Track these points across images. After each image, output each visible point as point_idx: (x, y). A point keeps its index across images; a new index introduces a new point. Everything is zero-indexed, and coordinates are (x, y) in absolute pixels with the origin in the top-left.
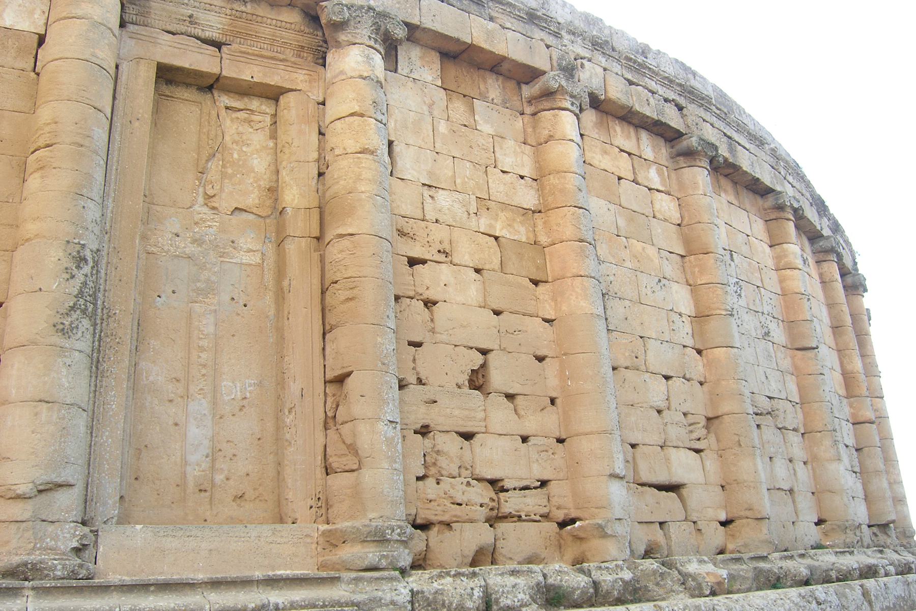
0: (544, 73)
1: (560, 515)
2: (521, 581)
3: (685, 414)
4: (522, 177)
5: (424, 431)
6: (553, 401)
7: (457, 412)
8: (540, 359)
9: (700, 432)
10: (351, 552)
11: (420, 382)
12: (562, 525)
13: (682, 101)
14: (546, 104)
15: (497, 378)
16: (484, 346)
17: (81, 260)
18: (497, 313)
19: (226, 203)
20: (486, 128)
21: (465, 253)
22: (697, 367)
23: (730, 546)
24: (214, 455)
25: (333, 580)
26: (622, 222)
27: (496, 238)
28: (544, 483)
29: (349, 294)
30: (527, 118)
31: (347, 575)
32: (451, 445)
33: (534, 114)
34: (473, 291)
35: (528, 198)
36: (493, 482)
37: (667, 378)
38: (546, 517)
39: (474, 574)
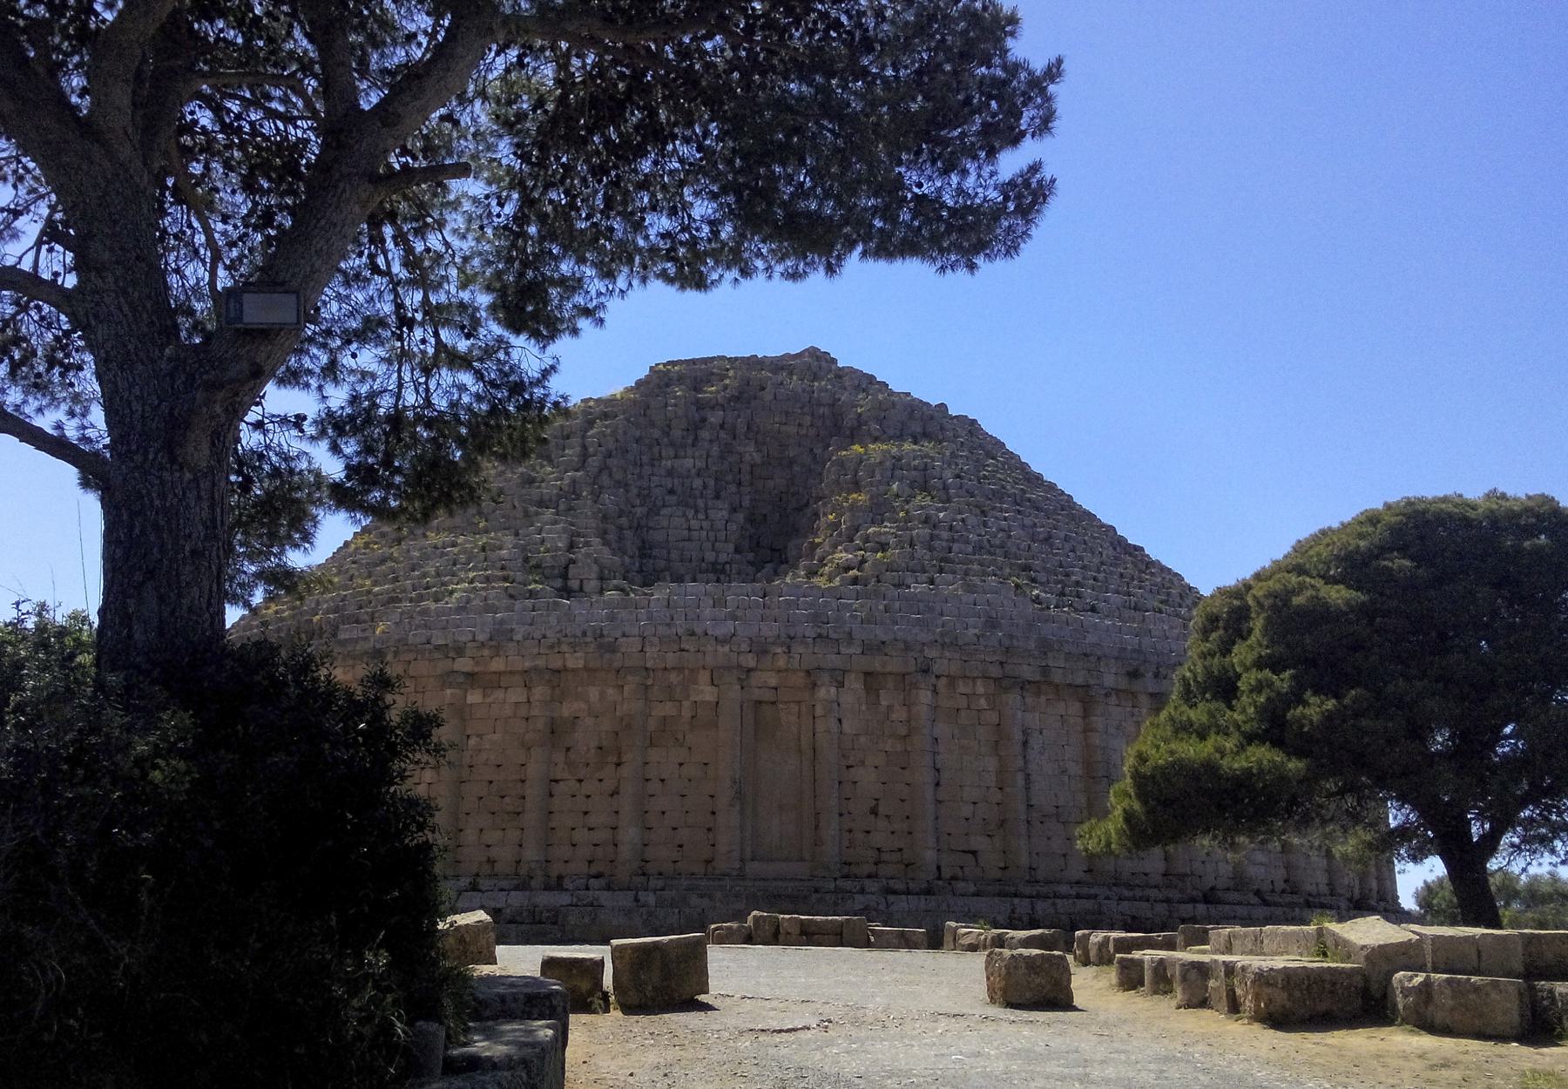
1: (906, 862)
2: (876, 884)
5: (850, 831)
8: (902, 801)
11: (849, 813)
12: (907, 866)
15: (881, 810)
16: (877, 797)
17: (735, 782)
20: (884, 703)
22: (998, 796)
28: (900, 850)
32: (860, 836)
35: (904, 732)
36: (878, 849)
37: (975, 803)
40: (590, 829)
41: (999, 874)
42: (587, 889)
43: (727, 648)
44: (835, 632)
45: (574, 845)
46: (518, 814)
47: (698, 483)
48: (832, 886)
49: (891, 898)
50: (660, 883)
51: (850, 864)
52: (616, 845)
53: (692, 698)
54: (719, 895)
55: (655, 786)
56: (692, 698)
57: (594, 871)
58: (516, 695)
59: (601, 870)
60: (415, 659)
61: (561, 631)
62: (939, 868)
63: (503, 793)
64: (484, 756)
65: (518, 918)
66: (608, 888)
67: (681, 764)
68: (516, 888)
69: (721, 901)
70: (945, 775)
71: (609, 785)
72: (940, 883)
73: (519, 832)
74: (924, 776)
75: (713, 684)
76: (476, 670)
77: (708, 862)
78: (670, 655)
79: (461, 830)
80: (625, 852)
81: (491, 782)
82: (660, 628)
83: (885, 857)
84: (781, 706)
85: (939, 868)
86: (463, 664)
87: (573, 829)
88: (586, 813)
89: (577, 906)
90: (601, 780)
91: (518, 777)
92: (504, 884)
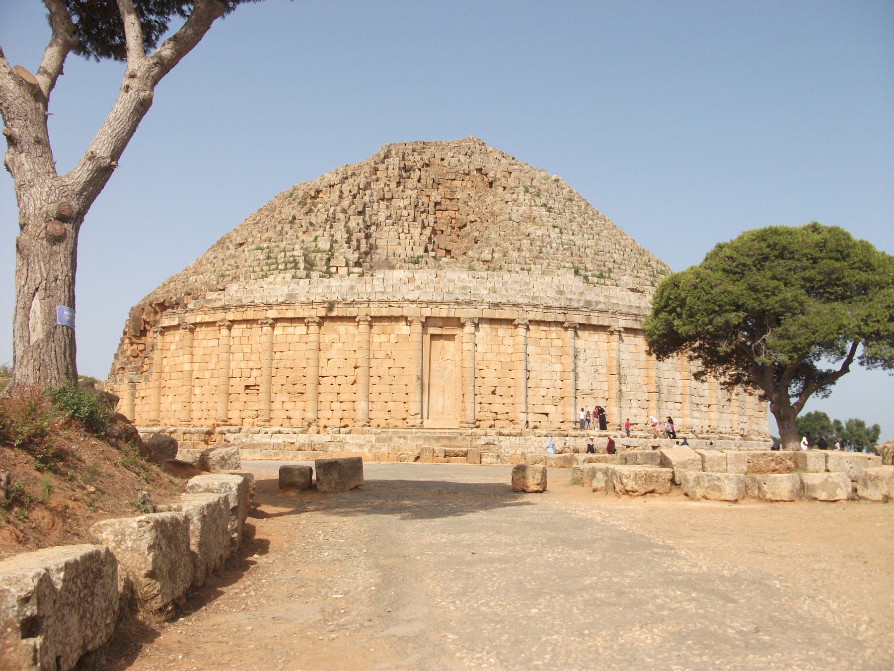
0: (515, 320)
5: (481, 403)
9: (557, 401)
10: (464, 425)
13: (566, 312)
15: (497, 392)
21: (492, 366)
22: (559, 384)
24: (443, 407)
26: (539, 351)
32: (486, 406)
34: (494, 374)
36: (496, 413)
41: (560, 425)
42: (339, 433)
43: (415, 305)
46: (303, 394)
47: (405, 213)
48: (471, 431)
49: (501, 438)
50: (379, 430)
51: (480, 421)
53: (396, 332)
54: (409, 436)
55: (375, 380)
56: (396, 332)
57: (343, 424)
58: (301, 329)
61: (324, 296)
62: (527, 422)
64: (284, 362)
65: (303, 448)
66: (350, 432)
68: (302, 432)
70: (532, 375)
71: (352, 379)
72: (527, 430)
74: (521, 375)
77: (404, 419)
78: (384, 309)
80: (360, 415)
82: (378, 295)
83: (499, 417)
85: (527, 422)
86: (272, 314)
88: (338, 394)
92: (296, 430)
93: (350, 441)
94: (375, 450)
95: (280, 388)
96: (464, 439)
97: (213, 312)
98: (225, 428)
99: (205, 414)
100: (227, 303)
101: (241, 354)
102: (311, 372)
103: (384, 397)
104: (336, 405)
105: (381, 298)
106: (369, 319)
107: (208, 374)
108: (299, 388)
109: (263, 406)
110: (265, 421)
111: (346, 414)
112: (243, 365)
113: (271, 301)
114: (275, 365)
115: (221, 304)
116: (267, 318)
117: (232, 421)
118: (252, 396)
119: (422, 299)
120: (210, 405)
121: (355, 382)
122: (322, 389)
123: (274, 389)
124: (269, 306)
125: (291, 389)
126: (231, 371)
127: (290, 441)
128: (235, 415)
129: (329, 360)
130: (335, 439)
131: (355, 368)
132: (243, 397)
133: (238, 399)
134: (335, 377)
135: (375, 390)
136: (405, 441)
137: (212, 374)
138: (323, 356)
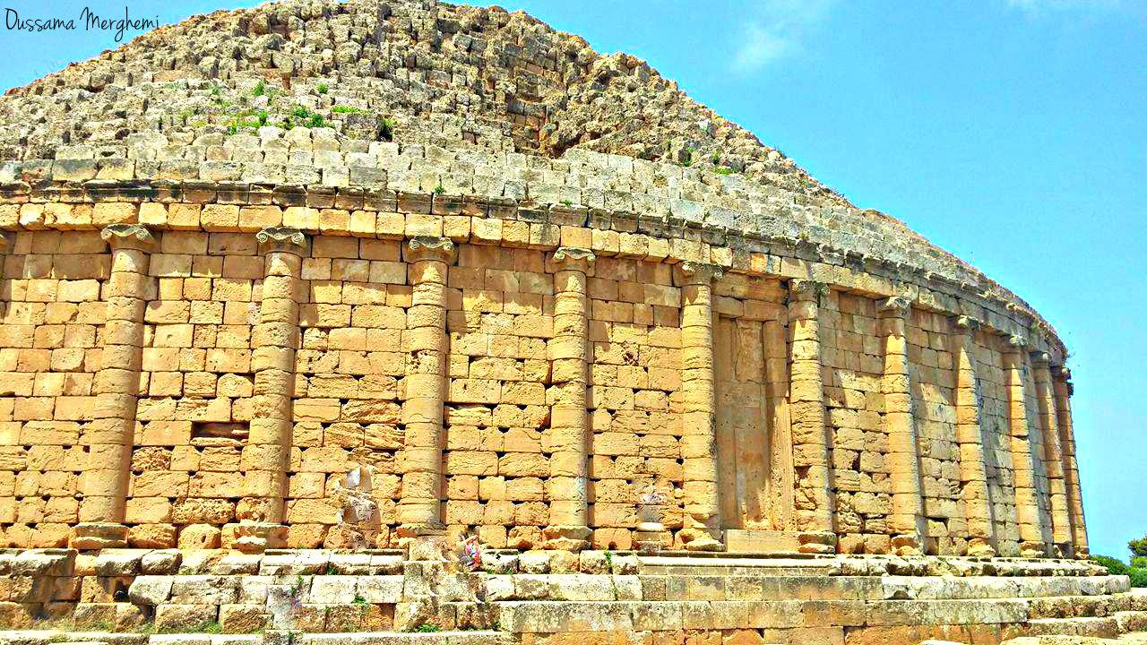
3: (950, 480)
4: (875, 356)
6: (888, 475)
7: (848, 482)
13: (959, 295)
14: (888, 315)
15: (863, 465)
16: (858, 449)
18: (864, 431)
19: (743, 379)
20: (859, 331)
23: (970, 551)
25: (813, 557)
27: (863, 392)
28: (884, 516)
29: (810, 430)
30: (878, 321)
31: (817, 555)
32: (845, 496)
33: (881, 319)
36: (864, 517)
38: (885, 532)
39: (863, 558)
40: (508, 478)
44: (815, 235)
45: (485, 502)
46: (392, 451)
52: (548, 503)
53: (647, 301)
54: (727, 578)
57: (513, 542)
59: (528, 539)
60: (214, 202)
63: (367, 418)
64: (329, 360)
67: (635, 391)
69: (732, 589)
71: (537, 414)
73: (394, 479)
75: (673, 285)
76: (324, 228)
77: (674, 529)
79: (294, 474)
80: (567, 516)
81: (344, 401)
84: (741, 325)
86: (302, 218)
87: (481, 477)
88: (500, 454)
89: (525, 599)
90: (522, 407)
91: (391, 396)
93: (572, 596)
94: (650, 624)
95: (317, 434)
96: (849, 586)
97: (87, 199)
98: (123, 557)
99: (30, 511)
100: (142, 177)
101: (184, 332)
102: (420, 387)
103: (619, 469)
104: (493, 487)
105: (618, 208)
106: (591, 257)
107: (51, 383)
108: (379, 434)
109: (261, 484)
110: (265, 533)
111: (524, 513)
112: (189, 360)
113: (297, 181)
114: (302, 367)
115: (126, 175)
116: (284, 230)
117: (139, 534)
118: (219, 452)
119: (711, 221)
120: (54, 481)
121: (546, 425)
122: (455, 438)
123: (299, 436)
124: (293, 196)
125: (354, 438)
126: (144, 377)
127: (379, 597)
128: (148, 513)
129: (472, 359)
130: (526, 589)
131: (548, 385)
132: (185, 458)
133: (165, 464)
134: (492, 406)
135: (601, 445)
136: (720, 592)
137: (71, 382)
138: (462, 346)
